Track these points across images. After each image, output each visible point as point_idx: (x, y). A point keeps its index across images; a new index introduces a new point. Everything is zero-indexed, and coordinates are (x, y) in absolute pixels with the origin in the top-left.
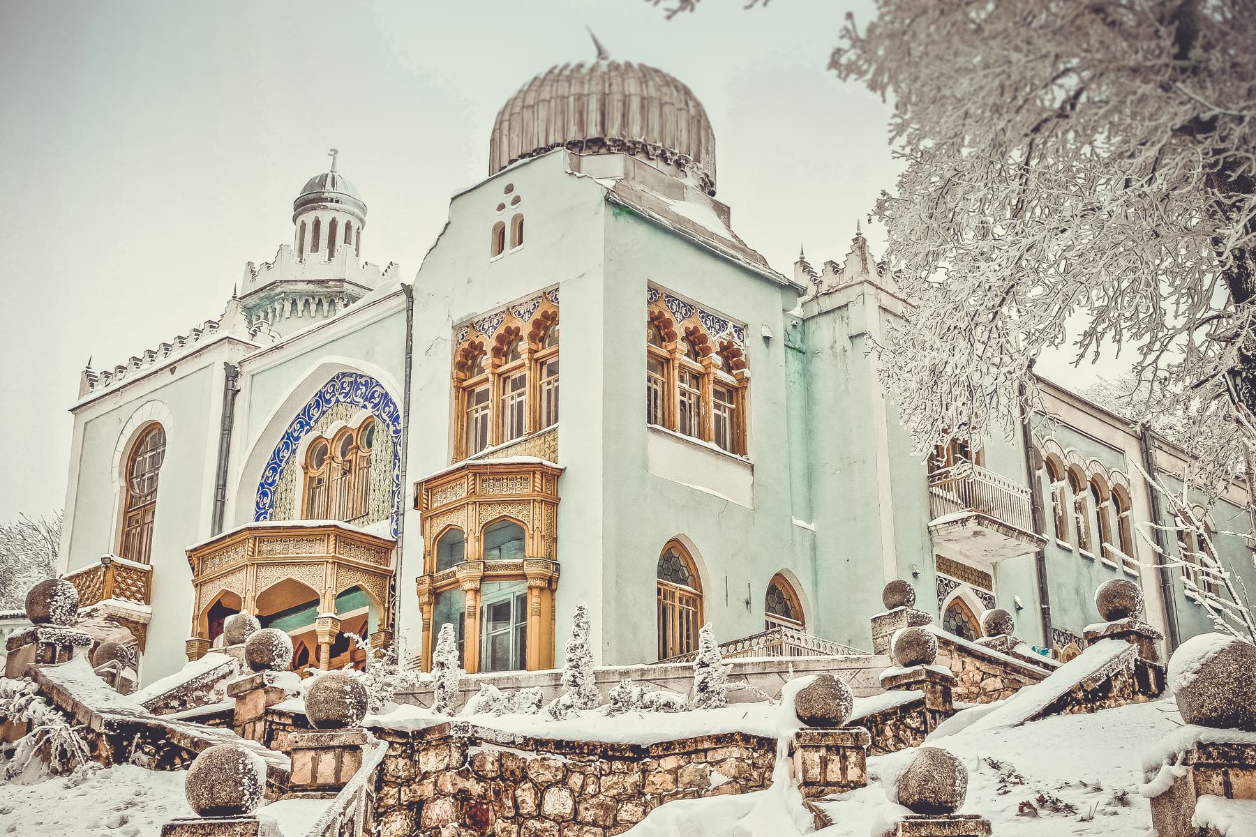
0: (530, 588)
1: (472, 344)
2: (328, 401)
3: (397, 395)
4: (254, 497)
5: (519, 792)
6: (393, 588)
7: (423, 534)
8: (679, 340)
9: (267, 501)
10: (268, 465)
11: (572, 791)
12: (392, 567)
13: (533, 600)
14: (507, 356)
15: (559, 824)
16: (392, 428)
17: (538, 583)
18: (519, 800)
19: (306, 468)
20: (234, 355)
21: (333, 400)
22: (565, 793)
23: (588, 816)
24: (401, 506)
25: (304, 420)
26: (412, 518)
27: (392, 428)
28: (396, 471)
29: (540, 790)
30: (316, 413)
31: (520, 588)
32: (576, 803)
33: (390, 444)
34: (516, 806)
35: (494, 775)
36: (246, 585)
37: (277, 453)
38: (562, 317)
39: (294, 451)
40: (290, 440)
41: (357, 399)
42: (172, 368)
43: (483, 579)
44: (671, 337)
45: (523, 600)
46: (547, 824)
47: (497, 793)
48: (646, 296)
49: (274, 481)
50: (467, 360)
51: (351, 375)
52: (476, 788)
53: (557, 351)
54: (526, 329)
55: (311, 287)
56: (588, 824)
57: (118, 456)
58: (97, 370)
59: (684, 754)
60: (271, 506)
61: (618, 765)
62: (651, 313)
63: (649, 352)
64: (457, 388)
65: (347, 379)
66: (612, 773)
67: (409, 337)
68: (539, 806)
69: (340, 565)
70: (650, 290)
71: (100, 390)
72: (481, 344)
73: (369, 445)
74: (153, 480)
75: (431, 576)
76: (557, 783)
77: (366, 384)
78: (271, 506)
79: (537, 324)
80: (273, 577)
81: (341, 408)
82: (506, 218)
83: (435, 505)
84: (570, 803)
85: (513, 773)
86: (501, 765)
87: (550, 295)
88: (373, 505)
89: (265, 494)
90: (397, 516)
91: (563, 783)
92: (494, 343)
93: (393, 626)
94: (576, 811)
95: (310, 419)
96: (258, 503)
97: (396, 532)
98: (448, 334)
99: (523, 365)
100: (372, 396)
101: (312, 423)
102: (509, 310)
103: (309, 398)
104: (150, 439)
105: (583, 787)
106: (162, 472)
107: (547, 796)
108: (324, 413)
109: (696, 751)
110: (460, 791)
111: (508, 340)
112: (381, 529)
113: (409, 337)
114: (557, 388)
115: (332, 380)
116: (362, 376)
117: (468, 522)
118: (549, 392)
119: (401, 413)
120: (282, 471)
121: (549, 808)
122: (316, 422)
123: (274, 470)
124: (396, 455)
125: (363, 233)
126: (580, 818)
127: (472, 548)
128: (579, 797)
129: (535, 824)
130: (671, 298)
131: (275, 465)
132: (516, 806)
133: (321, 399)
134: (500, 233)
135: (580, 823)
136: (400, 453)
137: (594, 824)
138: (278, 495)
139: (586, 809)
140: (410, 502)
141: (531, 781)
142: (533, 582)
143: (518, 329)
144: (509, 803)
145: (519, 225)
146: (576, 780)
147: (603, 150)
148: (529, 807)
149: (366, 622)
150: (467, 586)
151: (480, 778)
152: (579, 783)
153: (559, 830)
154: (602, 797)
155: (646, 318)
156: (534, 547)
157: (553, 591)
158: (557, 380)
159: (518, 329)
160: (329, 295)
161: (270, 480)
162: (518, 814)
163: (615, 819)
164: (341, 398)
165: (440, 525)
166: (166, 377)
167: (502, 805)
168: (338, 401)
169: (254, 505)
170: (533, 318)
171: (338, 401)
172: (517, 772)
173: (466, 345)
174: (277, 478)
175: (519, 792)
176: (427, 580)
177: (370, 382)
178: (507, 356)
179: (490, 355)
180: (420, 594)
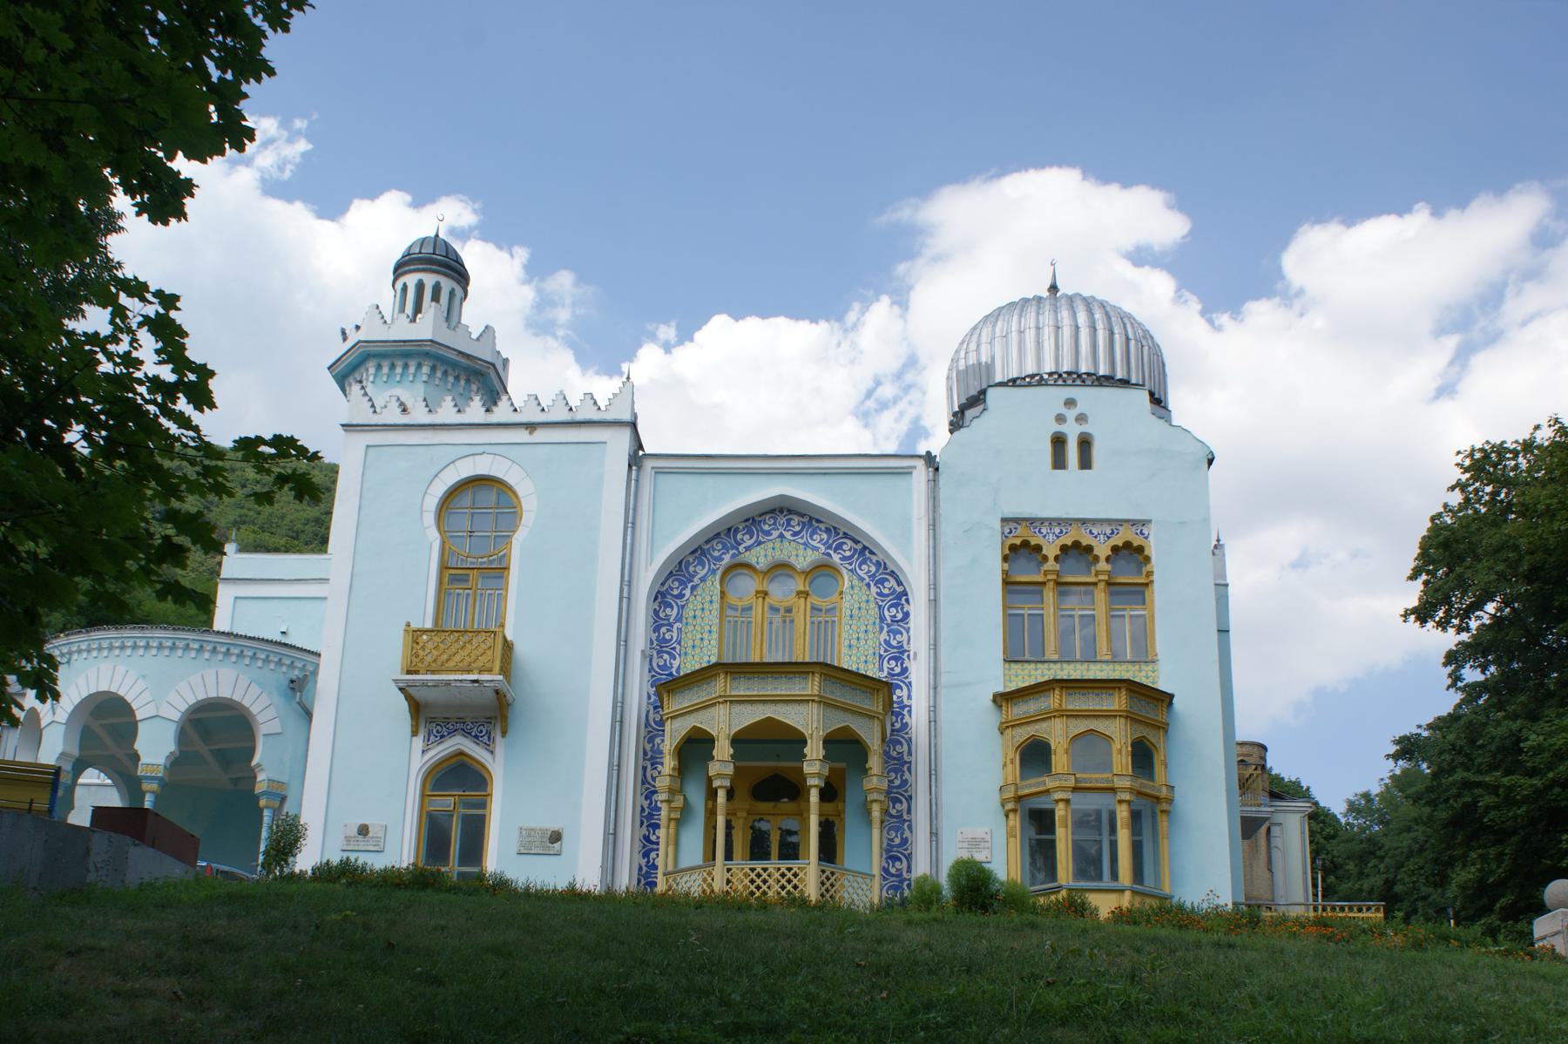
21: (775, 534)
33: (872, 605)
38: (1153, 550)
39: (714, 572)
49: (681, 596)
78: (679, 619)
82: (1072, 432)
115: (773, 511)
120: (694, 588)
122: (748, 549)
134: (1059, 442)
138: (689, 612)
145: (1085, 444)
164: (788, 535)
166: (522, 436)
168: (781, 536)
171: (781, 536)
173: (1018, 542)
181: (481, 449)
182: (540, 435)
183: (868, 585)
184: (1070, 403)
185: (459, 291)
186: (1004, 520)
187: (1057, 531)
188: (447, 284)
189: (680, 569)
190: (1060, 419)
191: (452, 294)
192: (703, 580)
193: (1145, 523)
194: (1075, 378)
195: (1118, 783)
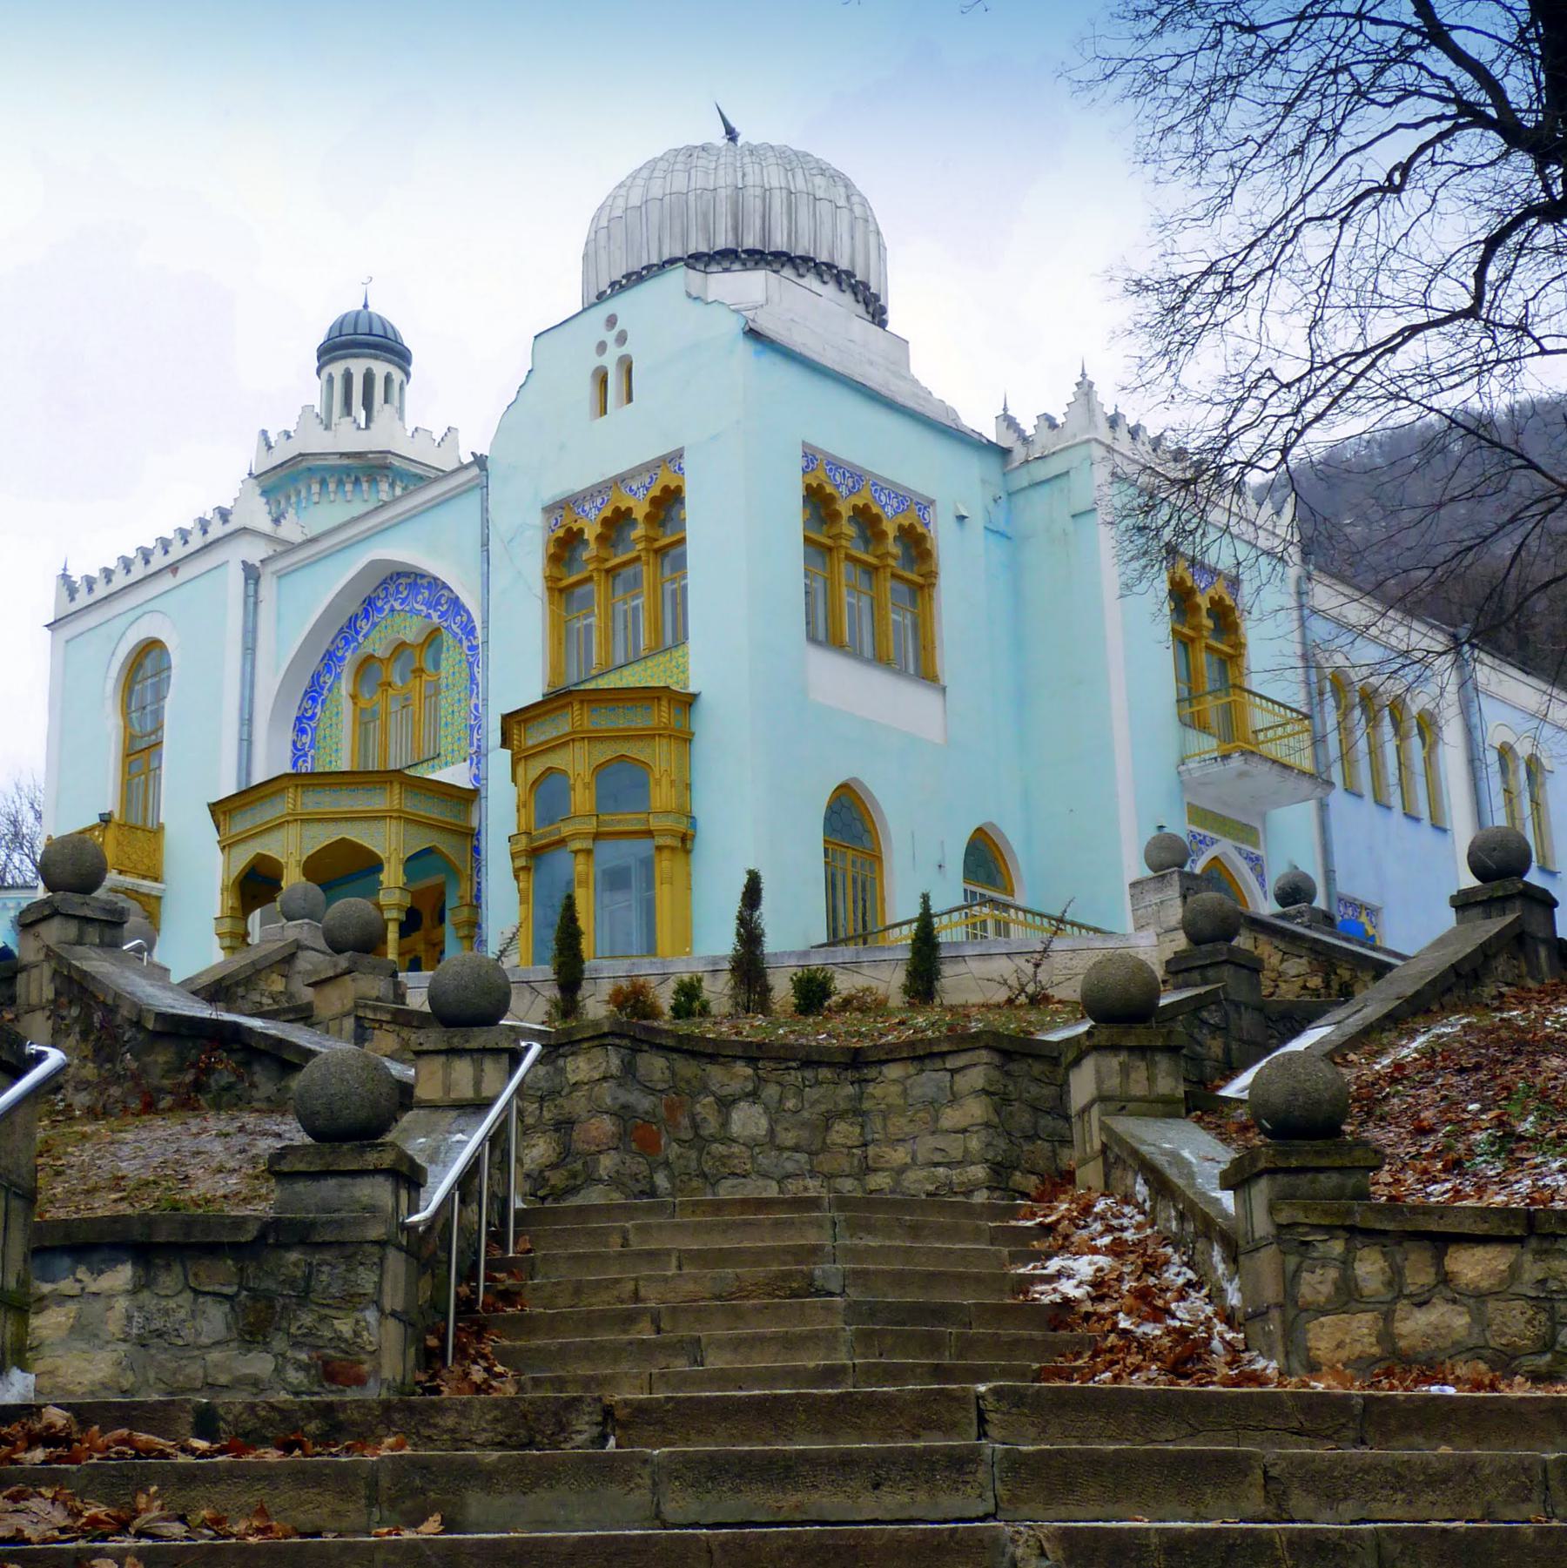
0: (659, 848)
1: (569, 530)
2: (380, 610)
3: (470, 601)
4: (290, 735)
5: (698, 1108)
6: (476, 850)
7: (514, 779)
8: (844, 521)
9: (306, 739)
10: (306, 692)
11: (767, 1109)
12: (475, 824)
13: (664, 864)
14: (619, 544)
15: (752, 1149)
16: (466, 644)
17: (669, 841)
18: (698, 1119)
19: (354, 697)
20: (255, 552)
21: (387, 607)
22: (758, 1109)
23: (789, 1138)
24: (483, 743)
25: (349, 631)
26: (500, 760)
27: (466, 644)
28: (474, 701)
29: (725, 1104)
30: (364, 626)
31: (643, 847)
32: (773, 1123)
33: (464, 665)
34: (695, 1126)
35: (665, 1086)
36: (291, 849)
37: (316, 677)
39: (338, 676)
40: (331, 659)
41: (418, 607)
42: (173, 568)
43: (597, 836)
44: (834, 516)
45: (648, 865)
46: (736, 1149)
47: (671, 1108)
48: (801, 463)
49: (314, 715)
50: (565, 547)
51: (407, 575)
52: (645, 1103)
53: (682, 541)
54: (641, 510)
55: (346, 462)
56: (788, 1149)
57: (110, 685)
58: (77, 577)
59: (913, 1059)
60: (311, 747)
61: (825, 1073)
62: (808, 488)
63: (807, 539)
64: (550, 589)
65: (402, 580)
66: (818, 1083)
67: (485, 523)
68: (725, 1124)
69: (408, 821)
70: (805, 455)
71: (83, 599)
72: (581, 531)
73: (437, 665)
74: (158, 717)
75: (528, 833)
76: (748, 1095)
77: (429, 587)
79: (655, 502)
80: (322, 837)
81: (398, 619)
82: (610, 361)
83: (530, 743)
84: (764, 1122)
85: (688, 1082)
86: (674, 1074)
87: (673, 460)
88: (445, 745)
89: (303, 731)
90: (478, 757)
91: (753, 1096)
92: (599, 530)
93: (478, 898)
94: (771, 1132)
95: (357, 633)
96: (294, 743)
97: (476, 778)
98: (538, 519)
99: (638, 558)
100: (438, 603)
101: (360, 639)
102: (620, 481)
103: (354, 607)
104: (146, 664)
105: (780, 1101)
106: (168, 703)
107: (735, 1116)
108: (374, 625)
109: (932, 1055)
110: (624, 1107)
111: (619, 521)
112: (456, 774)
113: (485, 523)
114: (685, 588)
115: (384, 582)
116: (423, 576)
117: (577, 763)
118: (674, 593)
119: (478, 623)
120: (323, 702)
121: (736, 1128)
122: (365, 636)
123: (314, 700)
124: (473, 679)
125: (407, 388)
126: (777, 1142)
127: (582, 799)
128: (775, 1114)
129: (717, 1148)
130: (835, 464)
131: (314, 693)
132: (695, 1126)
133: (369, 606)
135: (781, 1149)
136: (479, 677)
137: (796, 1149)
138: (320, 733)
139: (786, 1129)
140: (495, 736)
141: (713, 1093)
142: (660, 841)
143: (629, 510)
144: (686, 1122)
146: (771, 1091)
147: (736, 266)
148: (711, 1127)
149: (442, 894)
150: (577, 845)
151: (652, 1091)
152: (777, 1098)
153: (752, 1156)
154: (806, 1114)
155: (800, 492)
156: (662, 796)
157: (688, 852)
158: (685, 577)
159: (629, 510)
160: (370, 469)
161: (309, 714)
162: (697, 1135)
163: (824, 1142)
164: (397, 606)
165: (536, 768)
166: (167, 581)
167: (677, 1126)
169: (290, 747)
170: (652, 494)
171: (392, 610)
172: (695, 1083)
173: (561, 533)
174: (318, 710)
175: (698, 1108)
176: (524, 840)
177: (436, 584)
178: (619, 544)
179: (593, 545)
180: (514, 856)
181: (139, 612)
182: (185, 573)
183: (461, 641)
184: (611, 321)
185: (397, 375)
186: (548, 510)
187: (599, 501)
188: (380, 368)
189: (313, 685)
190: (602, 347)
191: (388, 379)
192: (330, 690)
193: (678, 455)
194: (618, 287)
195: (654, 824)
